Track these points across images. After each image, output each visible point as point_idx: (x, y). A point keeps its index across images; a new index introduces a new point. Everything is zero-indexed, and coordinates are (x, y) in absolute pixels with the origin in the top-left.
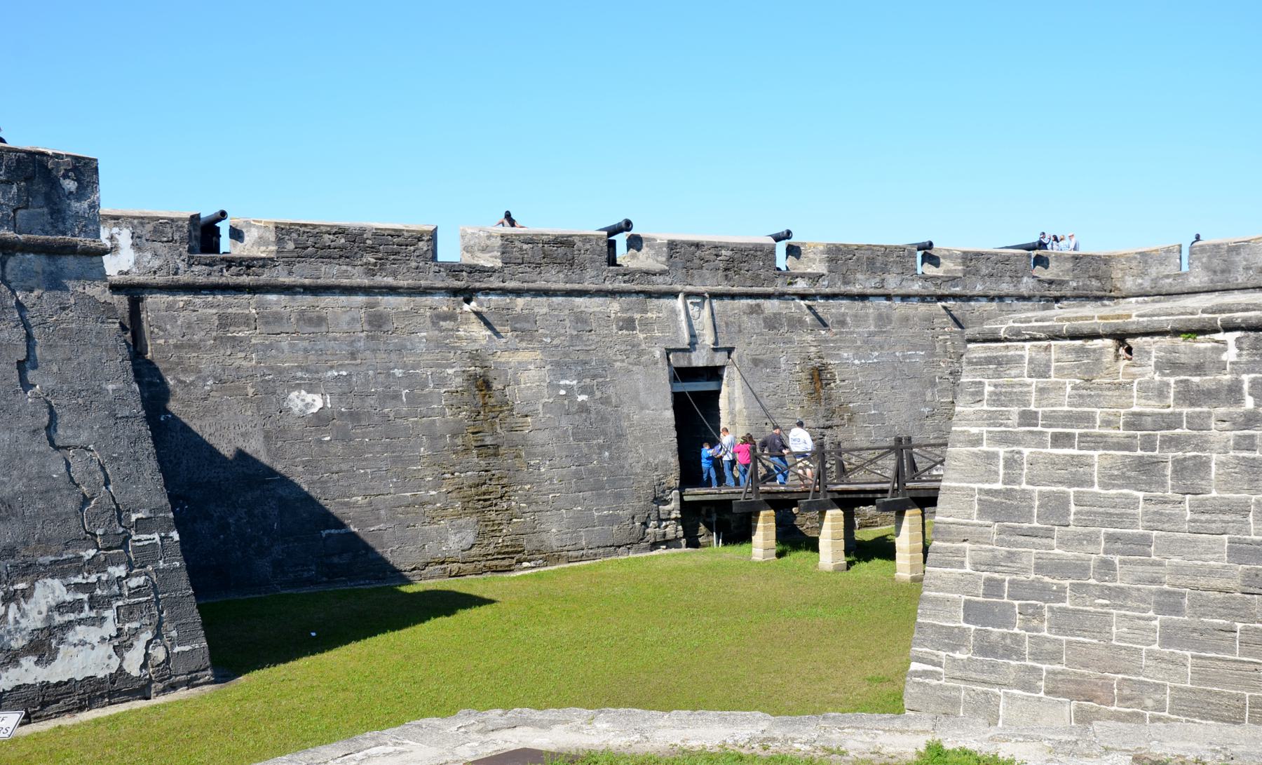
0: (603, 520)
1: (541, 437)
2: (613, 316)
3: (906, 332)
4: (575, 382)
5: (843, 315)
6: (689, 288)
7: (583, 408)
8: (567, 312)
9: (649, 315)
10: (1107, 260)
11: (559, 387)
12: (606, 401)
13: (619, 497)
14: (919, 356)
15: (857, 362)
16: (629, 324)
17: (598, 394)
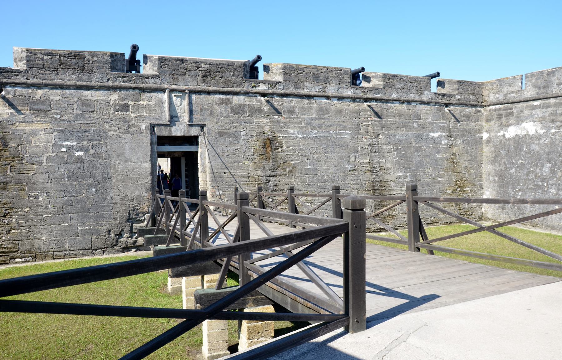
0: (84, 233)
1: (42, 178)
2: (112, 102)
3: (339, 119)
4: (75, 144)
5: (293, 107)
6: (174, 87)
7: (79, 160)
8: (76, 99)
9: (141, 102)
10: (480, 85)
11: (62, 146)
12: (97, 156)
13: (99, 218)
14: (347, 134)
15: (300, 136)
16: (125, 108)
17: (92, 151)
